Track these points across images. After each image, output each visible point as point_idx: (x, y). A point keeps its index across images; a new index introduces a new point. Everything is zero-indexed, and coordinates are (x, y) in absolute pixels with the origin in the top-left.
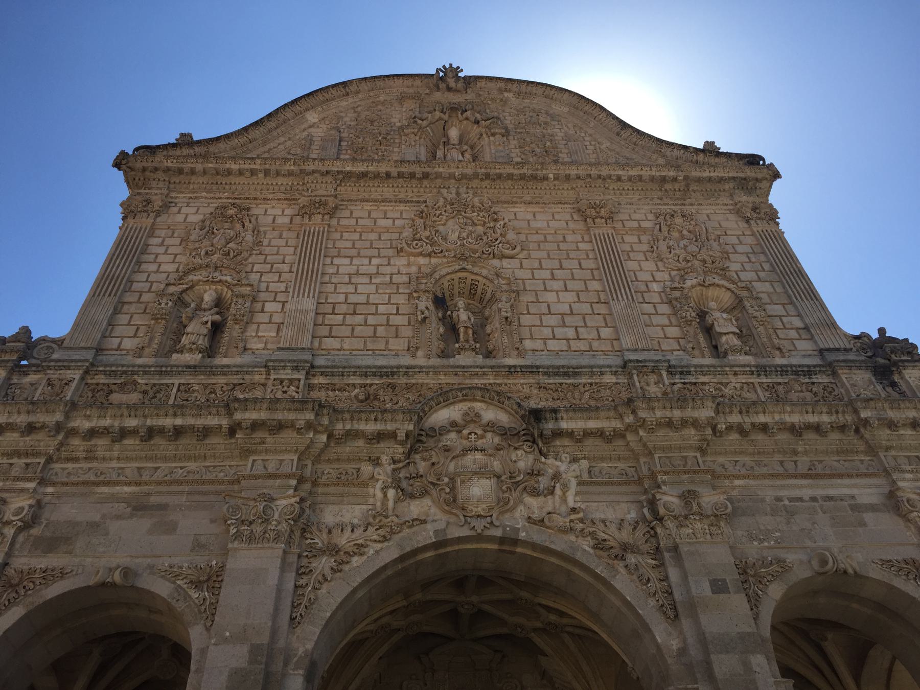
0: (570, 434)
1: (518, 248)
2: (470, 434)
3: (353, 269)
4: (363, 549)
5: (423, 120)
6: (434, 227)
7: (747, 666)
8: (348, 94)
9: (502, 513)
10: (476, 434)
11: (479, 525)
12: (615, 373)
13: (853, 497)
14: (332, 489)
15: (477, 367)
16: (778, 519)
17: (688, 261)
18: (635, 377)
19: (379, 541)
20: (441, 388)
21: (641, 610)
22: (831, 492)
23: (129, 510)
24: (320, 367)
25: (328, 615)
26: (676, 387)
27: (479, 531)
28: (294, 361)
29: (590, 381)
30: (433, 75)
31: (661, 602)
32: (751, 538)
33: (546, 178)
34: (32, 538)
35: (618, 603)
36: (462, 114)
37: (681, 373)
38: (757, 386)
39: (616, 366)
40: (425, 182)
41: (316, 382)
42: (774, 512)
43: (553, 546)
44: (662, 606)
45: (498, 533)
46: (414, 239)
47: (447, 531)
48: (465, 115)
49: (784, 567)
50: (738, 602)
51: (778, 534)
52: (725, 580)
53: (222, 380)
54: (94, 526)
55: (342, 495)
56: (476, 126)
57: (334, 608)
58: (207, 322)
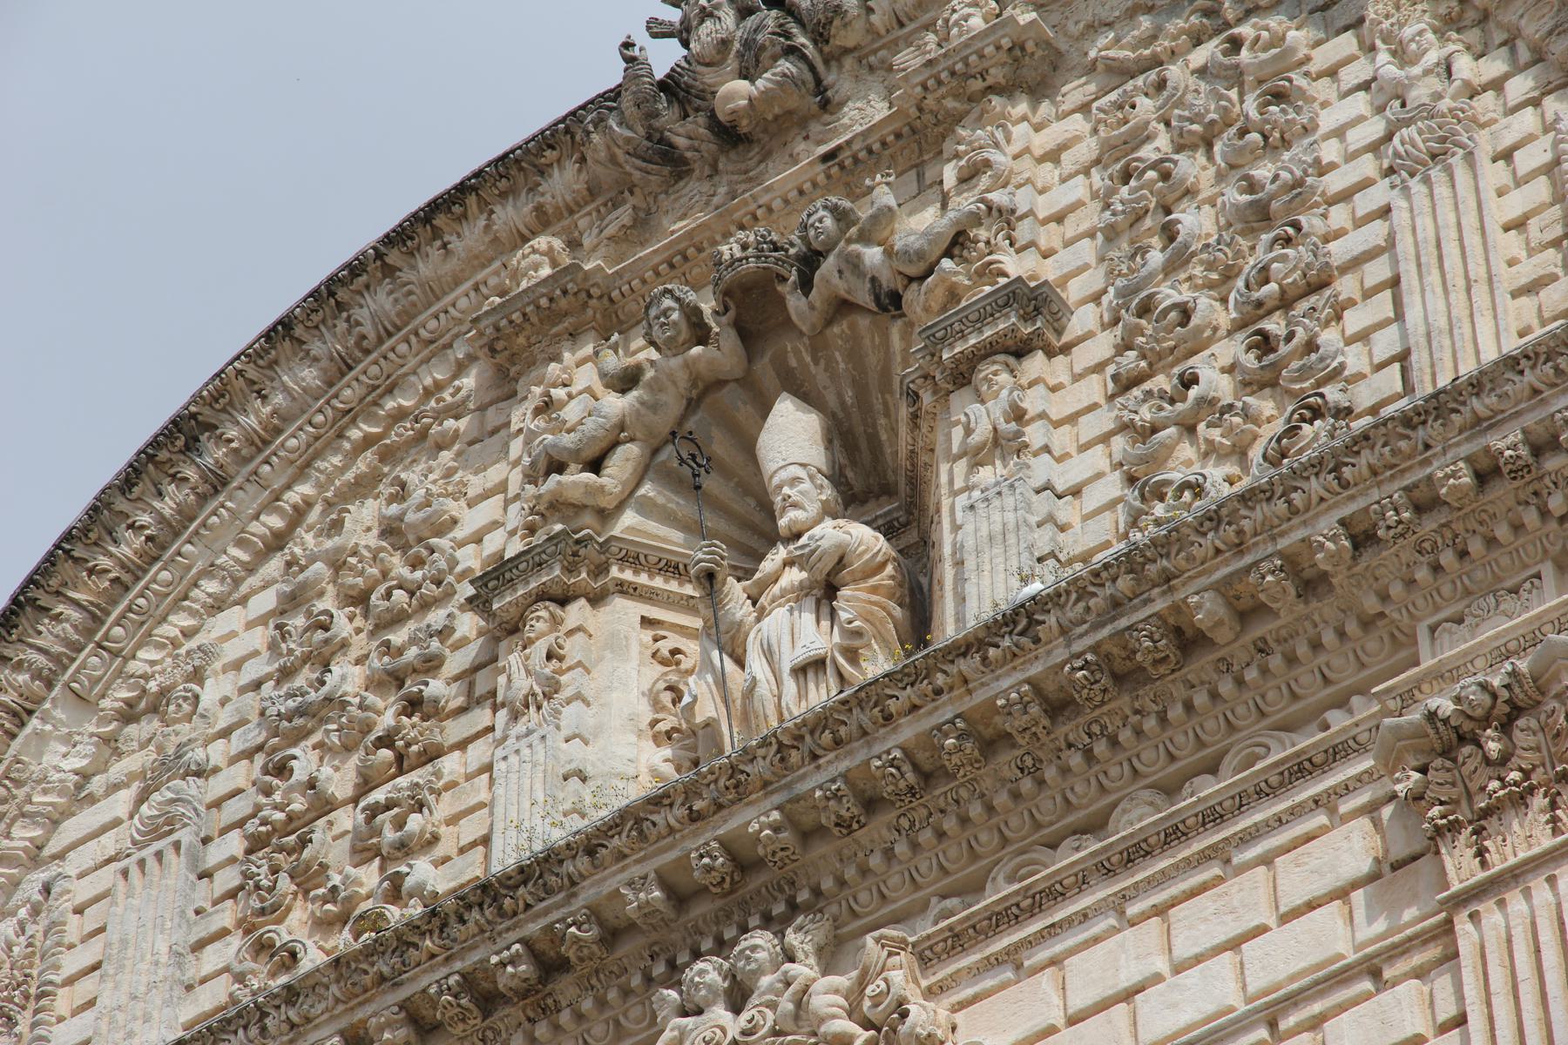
5: (595, 466)
8: (217, 483)
30: (615, 94)
40: (565, 988)
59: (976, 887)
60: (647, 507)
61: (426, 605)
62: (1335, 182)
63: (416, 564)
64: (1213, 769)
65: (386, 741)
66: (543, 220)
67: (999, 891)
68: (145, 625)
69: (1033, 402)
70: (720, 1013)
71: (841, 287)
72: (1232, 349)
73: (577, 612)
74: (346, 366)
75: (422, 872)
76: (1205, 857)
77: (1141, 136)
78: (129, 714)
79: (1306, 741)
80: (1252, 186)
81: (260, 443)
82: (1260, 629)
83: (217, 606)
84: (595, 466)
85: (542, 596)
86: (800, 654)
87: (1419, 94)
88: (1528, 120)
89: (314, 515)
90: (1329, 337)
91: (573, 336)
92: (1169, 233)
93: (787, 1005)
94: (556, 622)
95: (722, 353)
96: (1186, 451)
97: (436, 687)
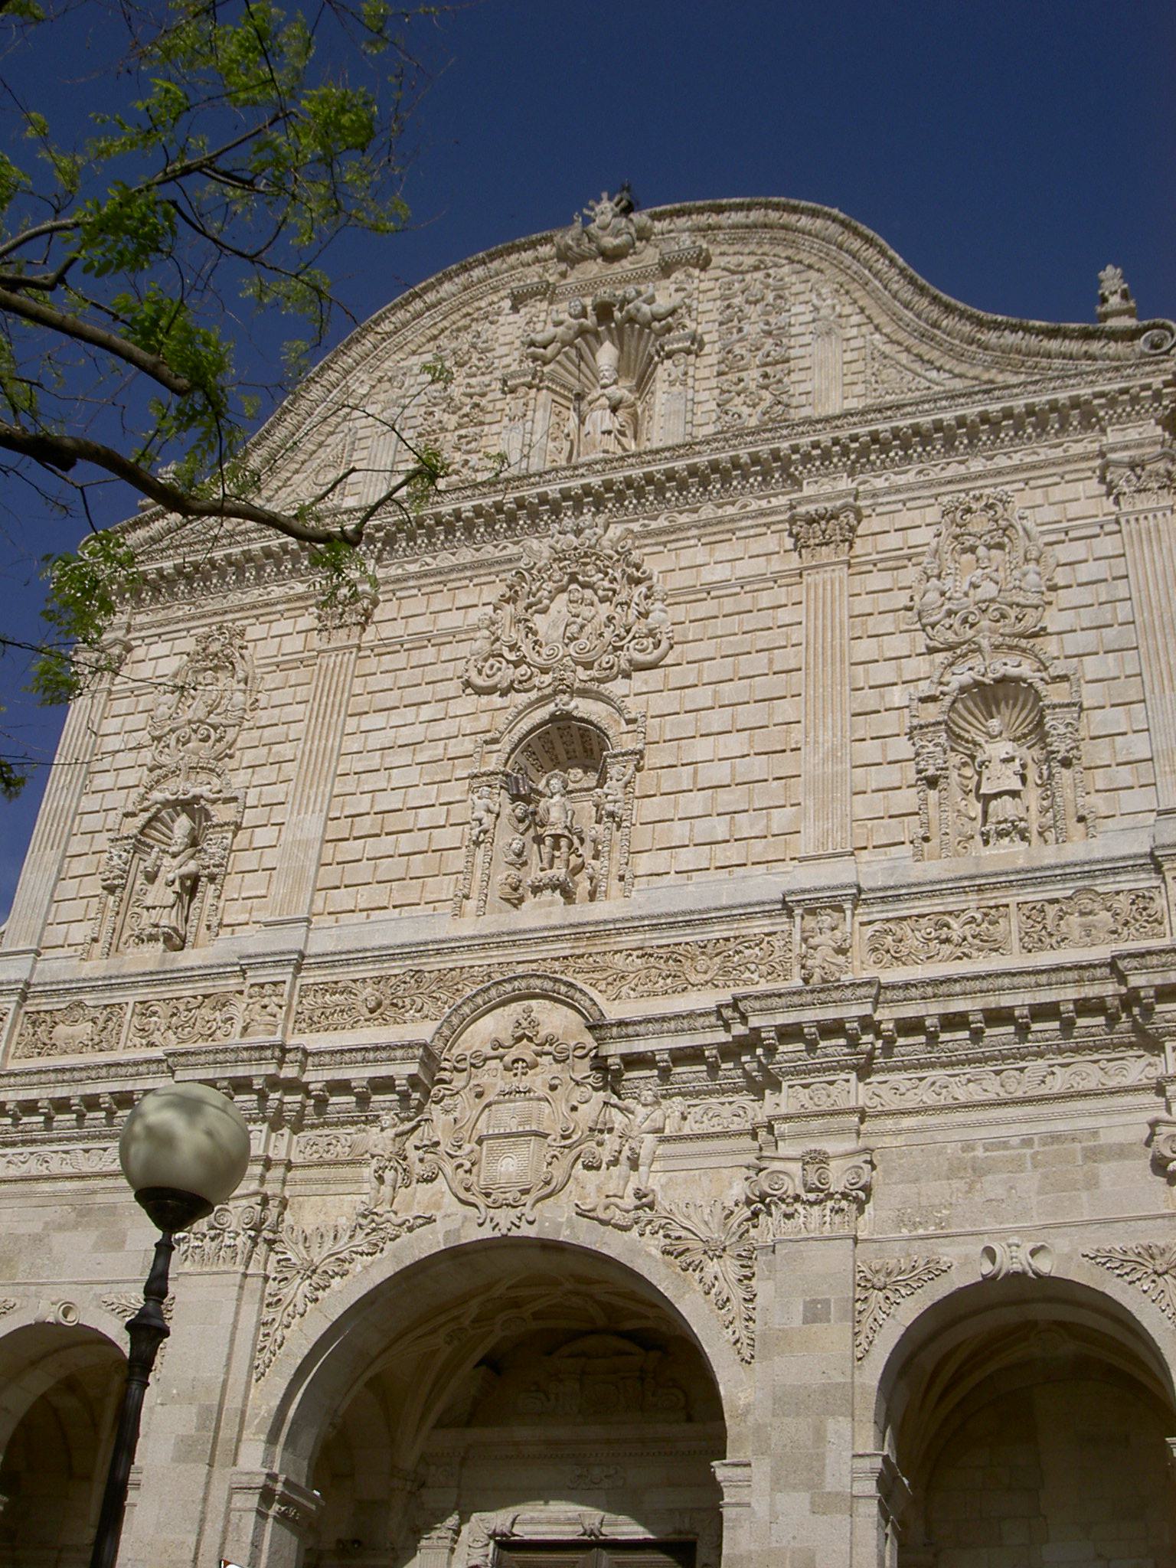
1: (664, 645)
2: (516, 1061)
4: (346, 1266)
5: (545, 348)
6: (527, 620)
7: (819, 1436)
10: (524, 1061)
11: (505, 1218)
12: (768, 914)
13: (1095, 1133)
14: (314, 1173)
15: (545, 929)
16: (956, 1184)
17: (972, 626)
19: (372, 1254)
20: (489, 975)
21: (710, 1347)
22: (1061, 1126)
23: (73, 1215)
25: (299, 1361)
26: (869, 930)
27: (504, 1231)
29: (726, 934)
31: (737, 1335)
32: (900, 1222)
36: (621, 310)
38: (1013, 908)
42: (953, 1173)
43: (605, 1251)
44: (737, 1341)
47: (463, 1233)
50: (836, 1335)
52: (827, 1302)
53: (186, 991)
54: (37, 1240)
57: (306, 1352)
58: (173, 882)
59: (655, 518)
61: (483, 374)
62: (794, 331)
63: (480, 359)
64: (733, 504)
65: (466, 415)
66: (537, 260)
67: (662, 522)
68: (389, 353)
70: (571, 536)
72: (756, 373)
74: (465, 289)
75: (473, 459)
76: (728, 531)
77: (734, 296)
78: (380, 380)
79: (764, 504)
80: (767, 323)
83: (414, 353)
84: (545, 348)
85: (523, 384)
86: (604, 428)
87: (823, 312)
88: (854, 332)
89: (447, 333)
90: (785, 380)
91: (541, 301)
93: (593, 541)
94: (527, 394)
95: (590, 322)
97: (483, 402)
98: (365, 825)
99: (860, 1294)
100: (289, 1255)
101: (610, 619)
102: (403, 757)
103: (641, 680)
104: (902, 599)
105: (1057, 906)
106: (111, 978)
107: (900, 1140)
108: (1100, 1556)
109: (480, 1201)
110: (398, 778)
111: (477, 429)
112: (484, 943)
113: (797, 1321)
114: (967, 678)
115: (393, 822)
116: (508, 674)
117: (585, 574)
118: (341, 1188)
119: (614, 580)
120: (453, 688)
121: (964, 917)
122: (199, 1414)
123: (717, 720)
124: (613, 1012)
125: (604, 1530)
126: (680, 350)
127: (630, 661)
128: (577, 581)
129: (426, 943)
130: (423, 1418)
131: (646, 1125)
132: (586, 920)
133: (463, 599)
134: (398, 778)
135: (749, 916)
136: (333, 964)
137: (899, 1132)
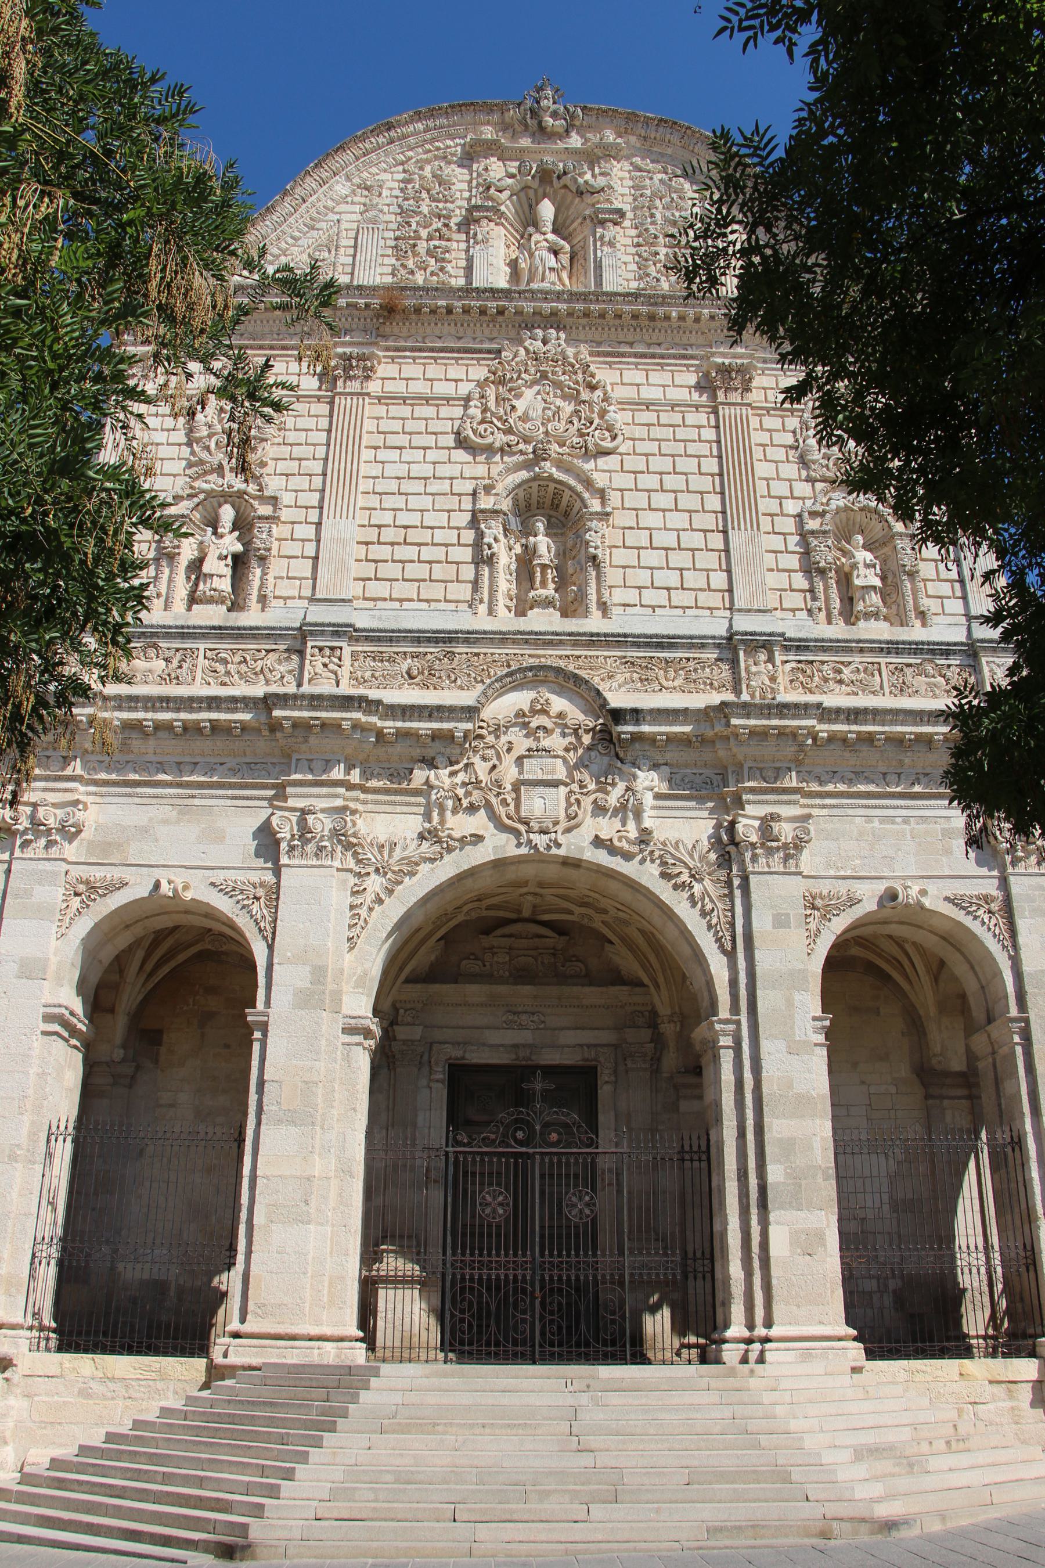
0: (651, 740)
1: (620, 438)
2: (538, 728)
3: (402, 470)
7: (790, 1003)
9: (568, 830)
10: (545, 728)
18: (741, 653)
23: (174, 813)
24: (365, 630)
26: (788, 667)
28: (334, 625)
29: (687, 655)
32: (828, 866)
33: (667, 318)
34: (85, 843)
35: (676, 933)
37: (798, 647)
39: (721, 638)
41: (360, 649)
45: (562, 852)
46: (483, 421)
48: (563, 181)
49: (853, 901)
50: (797, 936)
51: (858, 862)
54: (144, 831)
55: (394, 803)
56: (577, 200)
60: (507, 207)
61: (446, 201)
69: (618, 238)
70: (539, 343)
71: (569, 183)
73: (492, 224)
76: (658, 364)
77: (644, 187)
81: (404, 137)
82: (682, 324)
83: (385, 171)
92: (652, 216)
96: (653, 268)
98: (388, 535)
99: (808, 912)
100: (370, 856)
101: (577, 412)
102: (417, 487)
103: (602, 462)
104: (789, 440)
105: (911, 669)
106: (183, 627)
107: (825, 812)
108: (863, 1083)
109: (522, 828)
110: (414, 502)
111: (448, 244)
112: (502, 638)
113: (769, 927)
114: (841, 503)
115: (413, 536)
116: (500, 439)
117: (554, 373)
118: (405, 809)
119: (577, 383)
120: (450, 440)
121: (852, 667)
122: (312, 973)
123: (663, 500)
124: (617, 700)
125: (534, 1057)
126: (610, 220)
127: (596, 445)
128: (547, 378)
129: (457, 632)
130: (397, 977)
131: (647, 783)
132: (581, 630)
133: (452, 373)
134: (414, 502)
135: (703, 646)
136: (379, 640)
137: (824, 807)
